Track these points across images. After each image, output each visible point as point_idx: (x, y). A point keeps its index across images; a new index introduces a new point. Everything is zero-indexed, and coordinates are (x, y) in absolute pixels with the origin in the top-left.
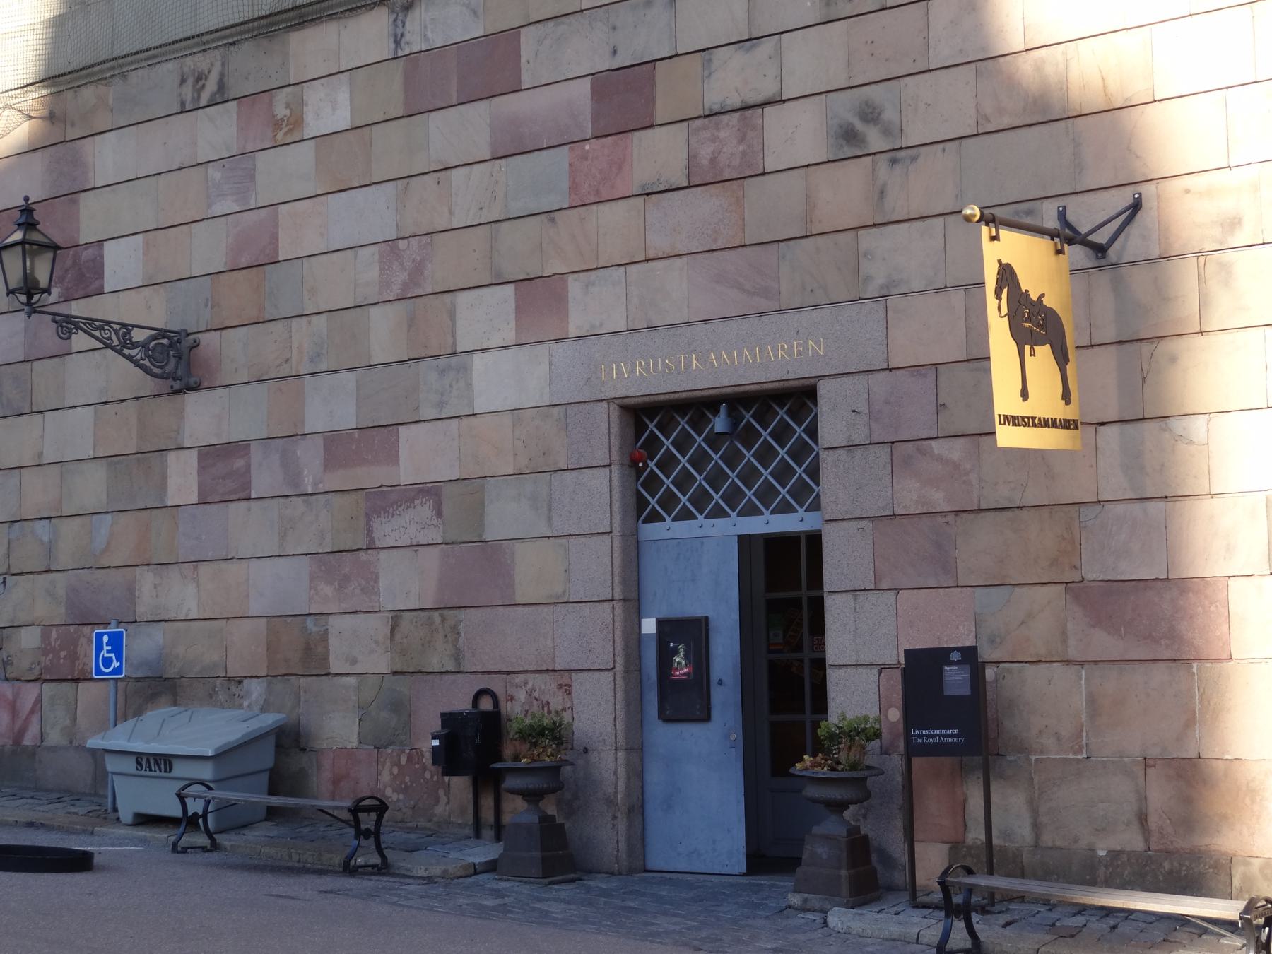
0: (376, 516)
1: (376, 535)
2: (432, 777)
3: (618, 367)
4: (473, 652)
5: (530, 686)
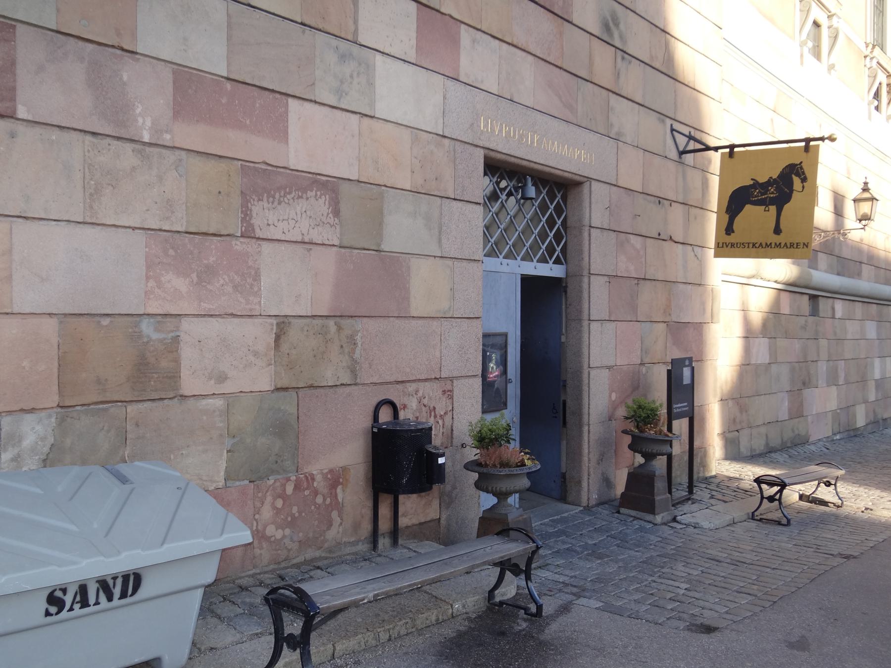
0: (256, 199)
1: (256, 221)
2: (324, 500)
3: (501, 125)
4: (370, 364)
5: (420, 394)
